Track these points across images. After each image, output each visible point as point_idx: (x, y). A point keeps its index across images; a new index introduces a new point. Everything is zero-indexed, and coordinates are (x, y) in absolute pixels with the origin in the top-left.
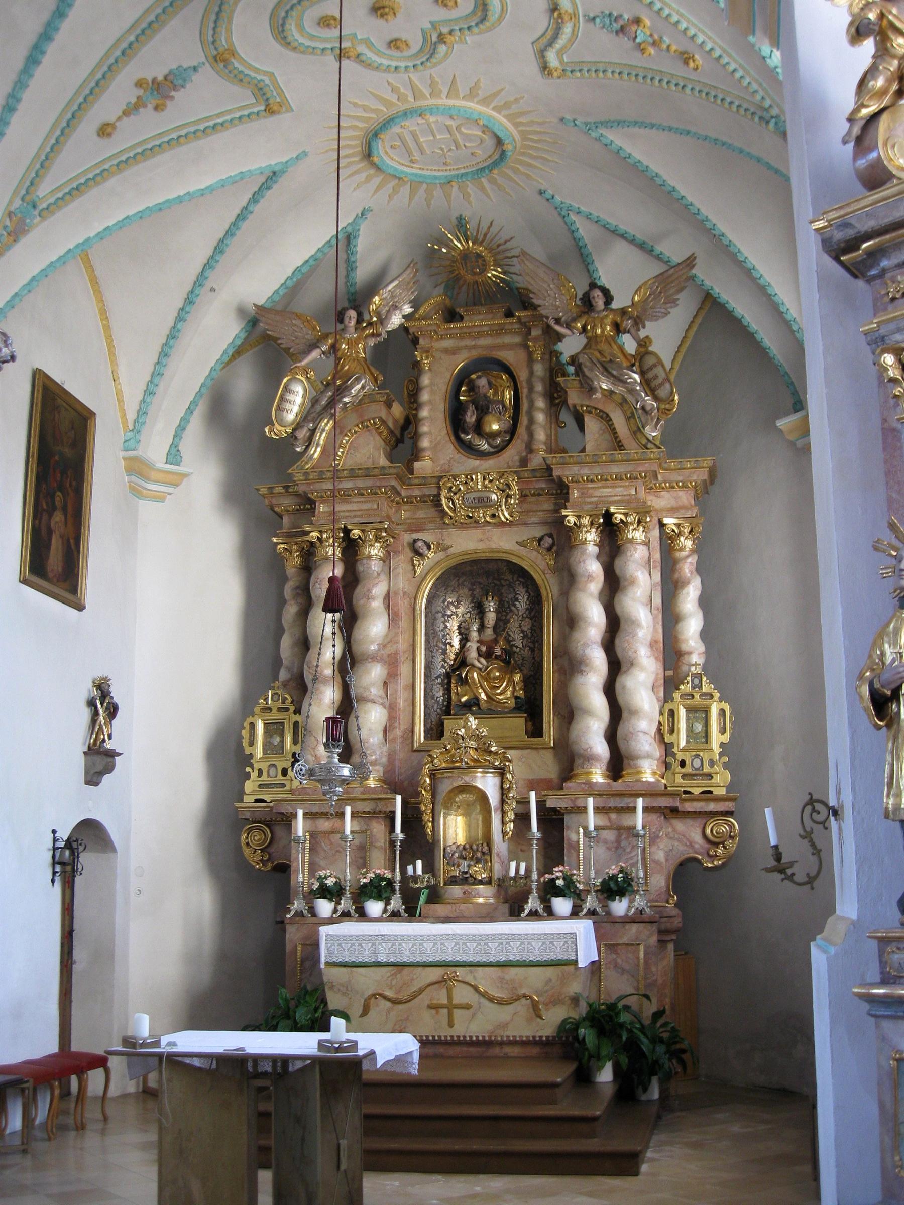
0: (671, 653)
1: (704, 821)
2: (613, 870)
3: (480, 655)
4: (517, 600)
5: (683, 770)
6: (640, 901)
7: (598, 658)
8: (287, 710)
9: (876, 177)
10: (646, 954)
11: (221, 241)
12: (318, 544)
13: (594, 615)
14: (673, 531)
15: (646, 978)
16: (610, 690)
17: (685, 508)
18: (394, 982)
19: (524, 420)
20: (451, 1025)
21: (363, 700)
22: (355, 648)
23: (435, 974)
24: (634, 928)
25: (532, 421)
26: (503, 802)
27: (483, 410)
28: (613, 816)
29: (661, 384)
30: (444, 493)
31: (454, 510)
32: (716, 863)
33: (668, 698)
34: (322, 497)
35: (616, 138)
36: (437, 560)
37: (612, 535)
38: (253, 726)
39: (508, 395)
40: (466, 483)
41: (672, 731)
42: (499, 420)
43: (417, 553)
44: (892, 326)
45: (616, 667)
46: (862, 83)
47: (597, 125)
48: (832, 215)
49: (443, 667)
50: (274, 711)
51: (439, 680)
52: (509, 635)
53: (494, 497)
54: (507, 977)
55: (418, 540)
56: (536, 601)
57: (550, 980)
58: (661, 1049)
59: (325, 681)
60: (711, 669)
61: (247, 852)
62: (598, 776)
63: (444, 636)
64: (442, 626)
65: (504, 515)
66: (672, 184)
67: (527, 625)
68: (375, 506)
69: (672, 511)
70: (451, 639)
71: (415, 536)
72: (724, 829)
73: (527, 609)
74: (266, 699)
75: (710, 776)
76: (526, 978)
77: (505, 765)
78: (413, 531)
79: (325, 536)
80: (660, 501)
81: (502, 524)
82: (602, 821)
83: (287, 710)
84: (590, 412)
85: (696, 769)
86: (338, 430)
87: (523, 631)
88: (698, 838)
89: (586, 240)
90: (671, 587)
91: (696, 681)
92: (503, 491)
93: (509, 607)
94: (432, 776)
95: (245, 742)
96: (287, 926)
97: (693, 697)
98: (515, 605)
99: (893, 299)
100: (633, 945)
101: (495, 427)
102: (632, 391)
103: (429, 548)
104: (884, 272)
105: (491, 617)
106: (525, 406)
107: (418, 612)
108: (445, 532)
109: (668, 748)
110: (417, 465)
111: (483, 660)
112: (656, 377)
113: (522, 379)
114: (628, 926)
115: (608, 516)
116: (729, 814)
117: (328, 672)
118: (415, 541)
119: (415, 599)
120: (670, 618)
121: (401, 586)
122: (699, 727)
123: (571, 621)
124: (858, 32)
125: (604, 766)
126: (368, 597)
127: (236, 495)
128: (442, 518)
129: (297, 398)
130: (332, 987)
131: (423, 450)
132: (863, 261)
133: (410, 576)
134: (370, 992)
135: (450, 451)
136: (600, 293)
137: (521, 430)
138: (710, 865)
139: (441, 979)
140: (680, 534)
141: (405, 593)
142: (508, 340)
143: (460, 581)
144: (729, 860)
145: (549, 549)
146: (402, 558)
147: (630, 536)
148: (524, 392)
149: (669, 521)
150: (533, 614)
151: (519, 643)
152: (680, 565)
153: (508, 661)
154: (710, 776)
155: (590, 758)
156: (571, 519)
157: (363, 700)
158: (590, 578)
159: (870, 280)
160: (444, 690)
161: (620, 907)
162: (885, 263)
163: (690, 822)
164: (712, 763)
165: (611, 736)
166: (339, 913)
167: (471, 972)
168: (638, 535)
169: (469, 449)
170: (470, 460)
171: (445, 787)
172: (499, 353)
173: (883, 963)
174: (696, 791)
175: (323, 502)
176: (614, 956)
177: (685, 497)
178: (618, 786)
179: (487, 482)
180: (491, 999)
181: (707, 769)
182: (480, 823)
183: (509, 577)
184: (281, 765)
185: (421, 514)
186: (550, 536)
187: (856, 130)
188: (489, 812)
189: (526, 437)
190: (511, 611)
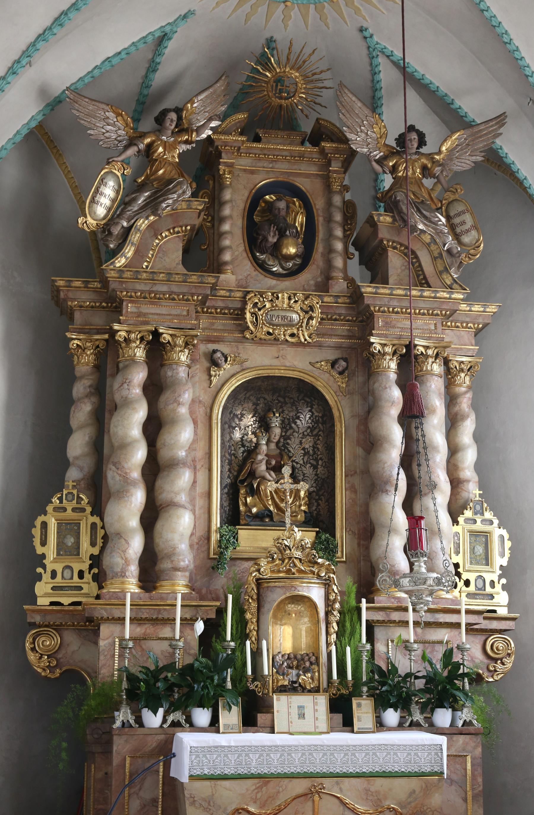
1: (484, 638)
4: (298, 418)
8: (83, 510)
10: (473, 765)
11: (64, 13)
12: (123, 345)
15: (473, 789)
18: (259, 796)
19: (319, 248)
23: (301, 786)
25: (330, 250)
26: (328, 613)
29: (468, 231)
30: (249, 306)
31: (256, 324)
32: (496, 678)
34: (131, 297)
36: (232, 372)
38: (44, 525)
39: (301, 219)
40: (272, 300)
42: (296, 245)
43: (215, 363)
52: (290, 451)
53: (295, 316)
54: (373, 789)
55: (217, 350)
57: (414, 791)
59: (134, 483)
61: (32, 657)
65: (303, 335)
66: (517, 45)
67: (308, 443)
68: (185, 313)
73: (309, 427)
75: (492, 597)
76: (390, 790)
79: (133, 336)
81: (300, 344)
83: (83, 510)
84: (395, 248)
85: (479, 589)
86: (154, 230)
87: (304, 449)
89: (383, 84)
91: (478, 507)
92: (307, 312)
93: (289, 424)
95: (37, 542)
96: (115, 738)
97: (475, 522)
101: (292, 250)
102: (440, 233)
107: (214, 421)
108: (241, 346)
111: (272, 473)
112: (463, 223)
113: (317, 207)
117: (136, 475)
118: (214, 351)
122: (480, 550)
123: (370, 443)
128: (242, 332)
129: (107, 194)
130: (193, 803)
133: (206, 384)
134: (234, 807)
135: (247, 267)
136: (416, 137)
138: (491, 680)
139: (307, 791)
141: (200, 402)
143: (248, 395)
145: (341, 373)
148: (320, 220)
154: (492, 597)
160: (230, 500)
166: (169, 722)
167: (337, 783)
169: (262, 267)
170: (267, 279)
172: (295, 179)
175: (132, 302)
179: (292, 302)
181: (488, 589)
183: (295, 395)
184: (77, 567)
186: (345, 360)
190: (291, 428)
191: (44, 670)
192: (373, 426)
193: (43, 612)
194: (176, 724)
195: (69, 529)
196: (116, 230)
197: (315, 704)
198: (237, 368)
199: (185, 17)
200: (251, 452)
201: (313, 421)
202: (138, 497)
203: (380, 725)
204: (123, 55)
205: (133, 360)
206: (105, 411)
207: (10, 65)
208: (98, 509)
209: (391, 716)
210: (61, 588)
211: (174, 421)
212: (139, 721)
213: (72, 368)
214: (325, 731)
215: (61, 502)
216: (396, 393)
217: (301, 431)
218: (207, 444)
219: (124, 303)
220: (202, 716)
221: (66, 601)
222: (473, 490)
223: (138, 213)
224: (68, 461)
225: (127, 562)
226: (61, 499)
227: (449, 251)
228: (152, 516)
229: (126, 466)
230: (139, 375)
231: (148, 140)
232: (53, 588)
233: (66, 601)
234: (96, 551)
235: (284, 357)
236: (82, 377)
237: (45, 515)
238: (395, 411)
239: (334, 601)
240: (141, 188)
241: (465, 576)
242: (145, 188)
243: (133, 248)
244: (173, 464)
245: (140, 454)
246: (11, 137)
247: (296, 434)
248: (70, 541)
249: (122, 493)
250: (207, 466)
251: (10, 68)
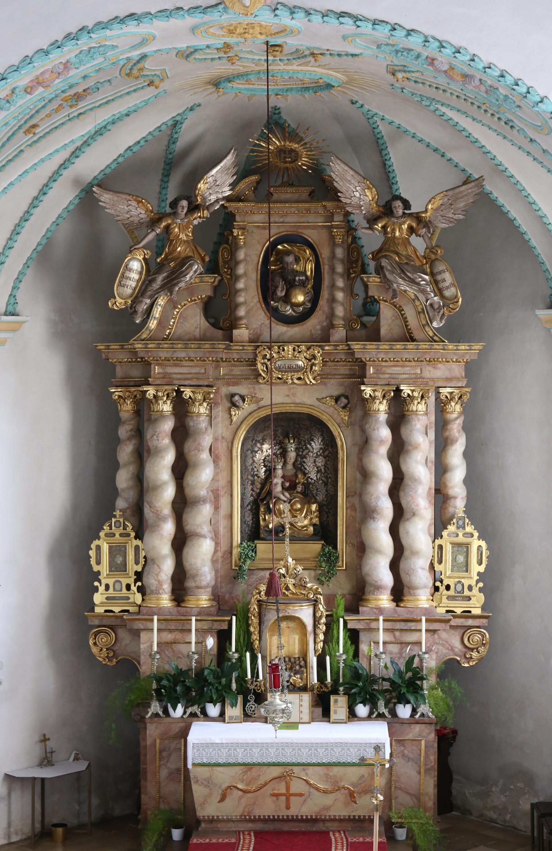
0: (441, 496)
1: (463, 631)
3: (283, 488)
5: (449, 593)
7: (386, 507)
10: (426, 747)
12: (154, 401)
13: (384, 470)
14: (446, 397)
15: (425, 765)
16: (394, 530)
18: (245, 777)
19: (325, 294)
20: (288, 807)
21: (198, 535)
22: (187, 491)
23: (276, 772)
24: (417, 728)
26: (315, 626)
27: (291, 286)
28: (397, 634)
29: (447, 288)
30: (259, 359)
32: (471, 664)
33: (437, 535)
34: (157, 360)
36: (250, 410)
38: (98, 548)
39: (310, 267)
40: (279, 352)
41: (440, 562)
42: (305, 294)
43: (234, 405)
45: (400, 514)
49: (252, 495)
50: (117, 536)
51: (249, 507)
52: (306, 469)
54: (331, 774)
56: (330, 444)
57: (363, 776)
59: (164, 519)
60: (469, 509)
61: (95, 650)
62: (384, 600)
63: (253, 469)
64: (251, 461)
65: (308, 378)
66: (476, 137)
67: (320, 462)
68: (203, 371)
70: (258, 471)
71: (233, 389)
73: (321, 448)
74: (110, 526)
75: (469, 598)
76: (345, 774)
77: (317, 598)
78: (228, 384)
85: (459, 592)
86: (172, 304)
90: (442, 445)
92: (310, 360)
93: (305, 445)
94: (260, 603)
95: (93, 561)
96: (148, 725)
97: (457, 535)
98: (310, 444)
101: (300, 298)
103: (244, 400)
105: (292, 455)
106: (326, 282)
107: (234, 454)
108: (257, 387)
109: (436, 578)
110: (235, 332)
111: (287, 494)
112: (444, 280)
113: (323, 256)
114: (413, 726)
115: (398, 391)
117: (167, 510)
119: (232, 444)
120: (441, 469)
121: (220, 431)
122: (461, 559)
125: (389, 592)
126: (199, 449)
127: (63, 331)
130: (197, 782)
131: (240, 318)
133: (227, 422)
134: (226, 785)
136: (401, 204)
137: (323, 303)
138: (466, 665)
139: (281, 775)
141: (223, 438)
142: (311, 218)
144: (480, 660)
145: (344, 407)
146: (220, 408)
147: (415, 409)
148: (326, 269)
150: (326, 453)
151: (313, 475)
152: (449, 427)
153: (307, 496)
154: (469, 598)
155: (378, 588)
156: (367, 391)
157: (198, 535)
160: (253, 515)
165: (395, 566)
166: (188, 713)
167: (304, 770)
168: (422, 407)
170: (278, 326)
171: (271, 617)
172: (303, 231)
174: (459, 611)
175: (158, 364)
176: (403, 748)
177: (458, 370)
179: (296, 353)
180: (317, 789)
181: (467, 593)
182: (297, 641)
184: (125, 581)
185: (237, 371)
186: (346, 397)
188: (305, 635)
189: (326, 309)
190: (307, 448)
191: (104, 659)
192: (365, 461)
193: (99, 616)
194: (193, 715)
195: (117, 551)
196: (143, 307)
197: (301, 700)
198: (254, 407)
199: (192, 109)
200: (270, 472)
201: (324, 443)
202: (169, 528)
203: (352, 715)
204: (142, 143)
205: (162, 415)
206: (142, 455)
207: (40, 188)
208: (139, 536)
209: (362, 710)
210: (113, 598)
211: (196, 465)
212: (166, 712)
213: (117, 412)
214: (308, 721)
215: (111, 529)
217: (315, 451)
218: (229, 474)
219: (152, 366)
220: (213, 710)
221: (117, 609)
222: (459, 505)
223: (158, 292)
224: (116, 489)
225: (160, 583)
226: (110, 526)
227: (431, 305)
228: (180, 542)
229: (157, 505)
230: (168, 425)
231: (164, 224)
232: (107, 598)
233: (117, 609)
234: (139, 568)
235: (294, 395)
236: (124, 423)
237: (99, 539)
238: (383, 450)
239: (321, 617)
240: (161, 267)
241: (445, 583)
242: (164, 271)
243: (155, 322)
244: (197, 502)
245: (169, 492)
246: (54, 220)
247: (311, 454)
248: (119, 560)
249: (156, 527)
250: (229, 492)
251: (41, 190)
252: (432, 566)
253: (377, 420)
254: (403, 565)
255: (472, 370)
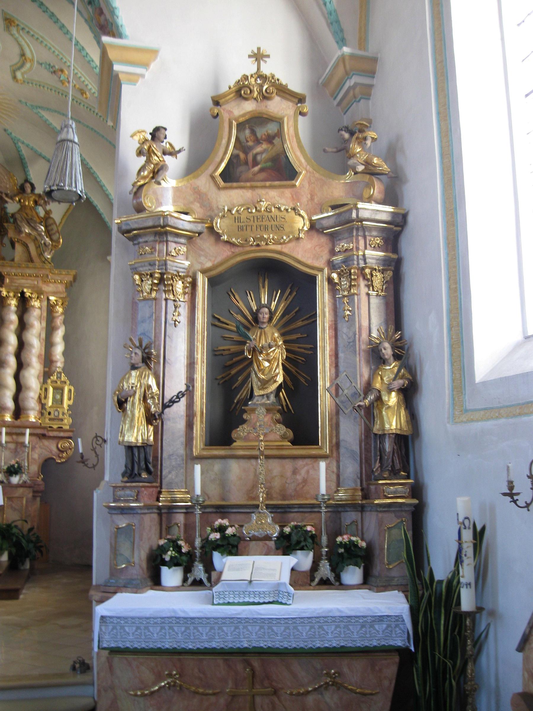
0: (48, 360)
2: (13, 462)
5: (50, 417)
6: (25, 477)
7: (12, 361)
9: (140, 209)
10: (27, 501)
13: (12, 340)
16: (17, 377)
17: (60, 293)
24: (21, 490)
28: (14, 437)
29: (55, 234)
32: (62, 460)
33: (45, 382)
35: (46, 115)
37: (24, 304)
44: (139, 265)
45: (21, 366)
46: (139, 171)
47: (37, 107)
48: (123, 219)
58: (31, 545)
62: (8, 418)
69: (54, 294)
72: (67, 445)
75: (62, 420)
80: (47, 288)
82: (9, 439)
84: (18, 242)
88: (54, 449)
90: (50, 330)
97: (56, 382)
99: (141, 254)
100: (21, 498)
102: (40, 235)
104: (139, 243)
109: (43, 406)
114: (18, 489)
115: (23, 293)
116: (70, 438)
120: (49, 344)
122: (58, 397)
124: (140, 153)
125: (11, 413)
132: (132, 238)
138: (59, 461)
140: (57, 304)
144: (68, 459)
147: (33, 304)
149: (52, 298)
152: (55, 320)
154: (62, 420)
158: (11, 322)
159: (134, 244)
161: (15, 480)
162: (141, 240)
163: (51, 441)
164: (63, 414)
165: (16, 399)
173: (114, 495)
174: (55, 427)
176: (11, 503)
177: (61, 288)
178: (18, 422)
181: (61, 416)
187: (135, 190)
216: (14, 317)
252: (40, 398)
253: (9, 310)
254: (21, 396)
255: (69, 286)
